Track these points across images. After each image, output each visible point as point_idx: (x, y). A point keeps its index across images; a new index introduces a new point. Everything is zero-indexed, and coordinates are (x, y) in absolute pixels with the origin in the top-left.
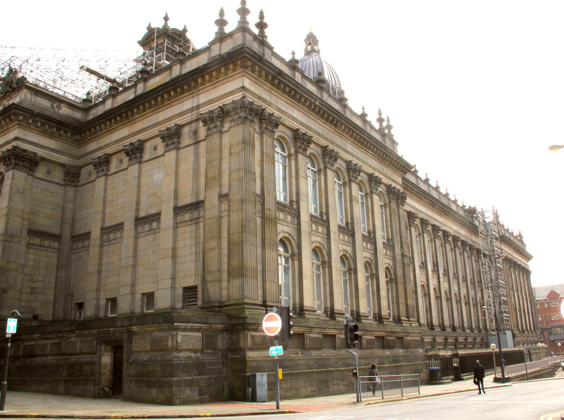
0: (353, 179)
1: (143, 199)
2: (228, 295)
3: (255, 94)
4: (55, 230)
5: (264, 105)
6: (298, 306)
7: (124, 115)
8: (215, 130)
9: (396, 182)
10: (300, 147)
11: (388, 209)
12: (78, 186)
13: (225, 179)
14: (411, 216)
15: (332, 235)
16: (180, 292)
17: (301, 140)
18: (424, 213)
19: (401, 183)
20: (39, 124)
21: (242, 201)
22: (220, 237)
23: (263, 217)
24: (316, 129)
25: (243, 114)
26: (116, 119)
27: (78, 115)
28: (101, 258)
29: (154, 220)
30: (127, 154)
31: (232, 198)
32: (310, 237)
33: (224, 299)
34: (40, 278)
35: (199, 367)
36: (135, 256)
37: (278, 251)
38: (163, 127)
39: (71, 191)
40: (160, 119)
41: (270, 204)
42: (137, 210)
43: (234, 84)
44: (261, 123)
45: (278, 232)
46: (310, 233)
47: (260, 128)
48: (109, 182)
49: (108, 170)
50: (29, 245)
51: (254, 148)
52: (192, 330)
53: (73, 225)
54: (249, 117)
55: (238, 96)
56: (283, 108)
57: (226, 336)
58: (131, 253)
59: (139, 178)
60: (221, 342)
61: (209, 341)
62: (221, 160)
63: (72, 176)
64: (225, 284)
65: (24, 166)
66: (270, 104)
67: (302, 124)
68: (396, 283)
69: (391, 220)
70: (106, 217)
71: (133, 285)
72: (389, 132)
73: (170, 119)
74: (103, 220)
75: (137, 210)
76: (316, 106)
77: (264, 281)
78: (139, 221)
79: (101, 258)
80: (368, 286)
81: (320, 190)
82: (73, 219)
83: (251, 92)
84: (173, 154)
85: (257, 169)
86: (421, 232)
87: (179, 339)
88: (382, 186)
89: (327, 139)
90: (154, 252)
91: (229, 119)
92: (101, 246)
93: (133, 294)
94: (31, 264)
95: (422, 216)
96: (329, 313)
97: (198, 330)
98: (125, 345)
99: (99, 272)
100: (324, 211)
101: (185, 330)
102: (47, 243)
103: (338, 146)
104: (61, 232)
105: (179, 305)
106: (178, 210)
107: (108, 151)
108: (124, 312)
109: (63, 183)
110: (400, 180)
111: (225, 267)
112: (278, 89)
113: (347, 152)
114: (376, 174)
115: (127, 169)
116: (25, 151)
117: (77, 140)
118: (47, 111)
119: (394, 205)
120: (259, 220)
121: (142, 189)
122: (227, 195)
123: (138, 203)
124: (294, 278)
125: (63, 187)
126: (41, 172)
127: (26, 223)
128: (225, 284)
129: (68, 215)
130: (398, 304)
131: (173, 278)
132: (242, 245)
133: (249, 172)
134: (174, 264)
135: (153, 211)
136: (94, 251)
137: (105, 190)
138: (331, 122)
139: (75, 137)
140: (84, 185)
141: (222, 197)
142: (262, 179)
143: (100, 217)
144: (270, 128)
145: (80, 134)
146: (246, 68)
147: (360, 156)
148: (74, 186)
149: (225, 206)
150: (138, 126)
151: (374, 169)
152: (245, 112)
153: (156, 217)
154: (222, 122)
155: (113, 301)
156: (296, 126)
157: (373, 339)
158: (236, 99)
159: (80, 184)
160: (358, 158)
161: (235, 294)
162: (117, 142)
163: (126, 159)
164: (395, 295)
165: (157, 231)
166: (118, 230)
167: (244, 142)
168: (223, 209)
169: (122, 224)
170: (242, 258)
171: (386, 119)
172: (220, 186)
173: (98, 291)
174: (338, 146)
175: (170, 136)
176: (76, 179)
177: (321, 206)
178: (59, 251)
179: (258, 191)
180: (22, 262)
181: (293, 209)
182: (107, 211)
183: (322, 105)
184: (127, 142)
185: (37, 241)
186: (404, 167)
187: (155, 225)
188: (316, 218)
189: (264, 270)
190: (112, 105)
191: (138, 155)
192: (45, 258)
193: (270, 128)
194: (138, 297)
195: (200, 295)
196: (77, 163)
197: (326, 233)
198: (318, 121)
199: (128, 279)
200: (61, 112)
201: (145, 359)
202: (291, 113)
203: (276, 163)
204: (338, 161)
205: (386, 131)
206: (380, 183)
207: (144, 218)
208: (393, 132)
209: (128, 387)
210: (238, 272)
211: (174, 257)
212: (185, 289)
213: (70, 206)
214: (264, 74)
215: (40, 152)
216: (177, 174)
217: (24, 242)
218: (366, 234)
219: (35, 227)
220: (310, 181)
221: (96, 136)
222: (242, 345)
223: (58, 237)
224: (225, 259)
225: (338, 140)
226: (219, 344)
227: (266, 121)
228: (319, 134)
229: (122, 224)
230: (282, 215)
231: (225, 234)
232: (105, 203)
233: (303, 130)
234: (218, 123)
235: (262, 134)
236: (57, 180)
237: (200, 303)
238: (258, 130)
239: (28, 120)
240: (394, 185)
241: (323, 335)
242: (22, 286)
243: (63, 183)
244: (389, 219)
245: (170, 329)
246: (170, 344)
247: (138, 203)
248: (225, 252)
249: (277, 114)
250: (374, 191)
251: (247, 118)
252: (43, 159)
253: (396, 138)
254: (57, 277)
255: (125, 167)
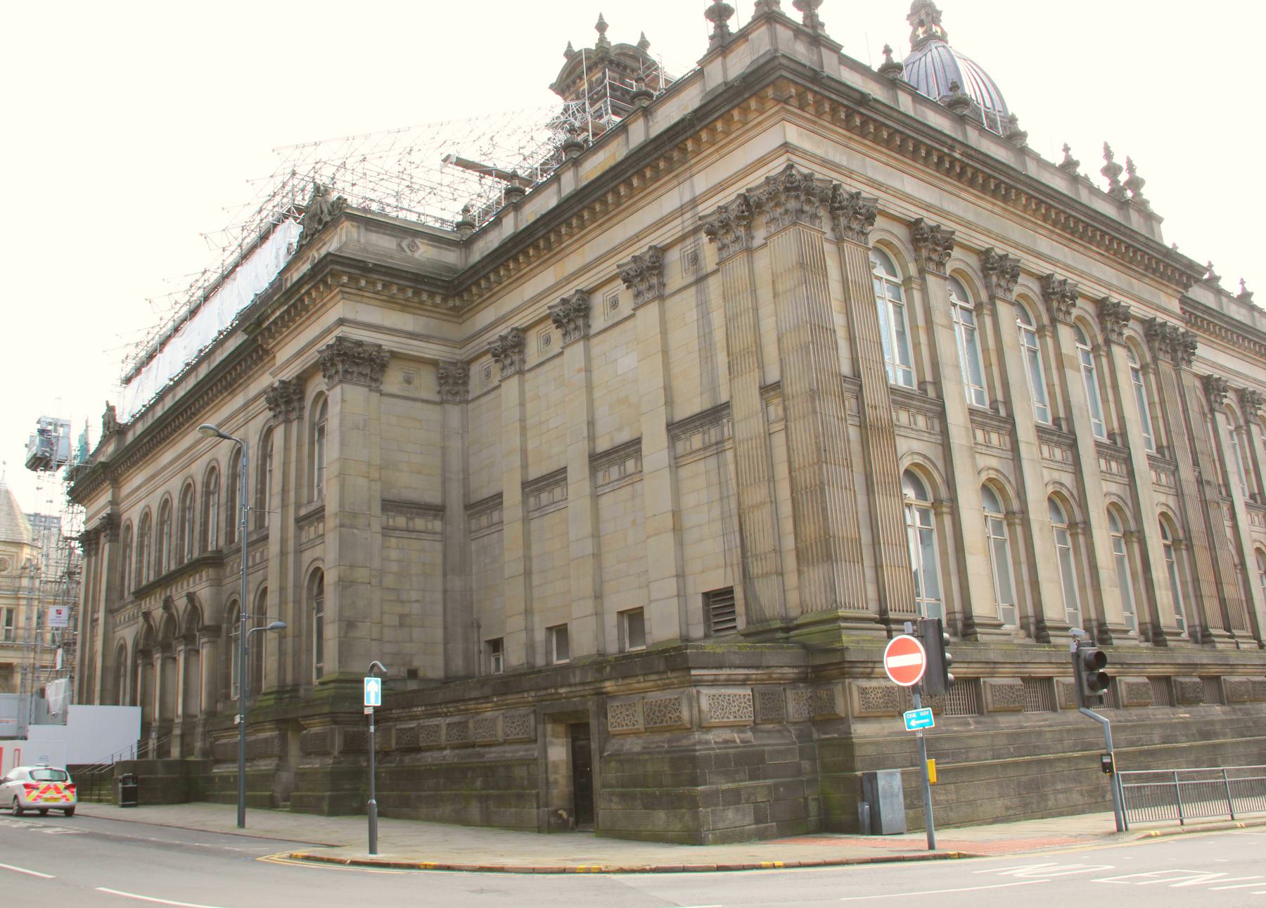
0: (1061, 316)
1: (602, 412)
2: (802, 603)
3: (814, 156)
4: (433, 497)
5: (836, 178)
6: (959, 616)
7: (542, 243)
8: (736, 247)
9: (1165, 311)
10: (930, 259)
11: (1152, 377)
12: (467, 402)
13: (771, 352)
14: (1211, 386)
15: (1023, 449)
16: (697, 603)
17: (928, 242)
18: (1246, 377)
19: (1178, 311)
20: (379, 287)
21: (813, 394)
22: (772, 479)
23: (863, 426)
24: (961, 214)
25: (792, 204)
26: (526, 254)
27: (451, 257)
28: (527, 545)
29: (628, 456)
30: (558, 323)
31: (788, 390)
32: (973, 458)
33: (794, 612)
34: (414, 595)
35: (749, 762)
36: (596, 535)
37: (902, 496)
38: (625, 257)
39: (454, 412)
40: (617, 241)
41: (875, 394)
42: (592, 438)
43: (766, 142)
44: (834, 218)
45: (899, 455)
46: (973, 450)
47: (833, 230)
48: (528, 386)
49: (523, 361)
50: (387, 531)
51: (826, 275)
52: (729, 682)
53: (465, 482)
54: (806, 208)
55: (776, 167)
56: (880, 178)
57: (804, 691)
58: (587, 529)
59: (588, 370)
60: (795, 705)
61: (768, 707)
62: (756, 310)
63: (453, 381)
64: (792, 580)
65: (360, 374)
66: (850, 173)
67: (928, 207)
68: (1190, 548)
69: (1162, 402)
70: (530, 459)
71: (598, 596)
72: (1137, 194)
73: (638, 237)
74: (525, 467)
75: (592, 438)
76: (953, 161)
77: (878, 567)
78: (597, 460)
79: (527, 545)
80: (1120, 561)
81: (985, 350)
82: (465, 470)
83: (805, 154)
84: (652, 310)
85: (839, 320)
86: (1242, 422)
87: (704, 704)
88: (1131, 323)
89: (987, 233)
90: (634, 523)
91: (764, 219)
92: (526, 520)
93: (599, 614)
94: (394, 567)
95: (1239, 383)
96: (1032, 628)
97: (743, 683)
98: (593, 722)
99: (528, 573)
100: (1000, 397)
101: (714, 683)
102: (419, 523)
103: (1017, 246)
104: (444, 500)
105: (698, 631)
106: (676, 429)
107: (519, 321)
108: (585, 653)
109: (437, 398)
110: (1175, 306)
111: (789, 542)
112: (864, 137)
113: (1039, 255)
114: (1115, 298)
115: (561, 353)
116: (359, 344)
117: (454, 308)
118: (391, 257)
119: (1165, 366)
120: (853, 433)
121: (597, 394)
122: (777, 386)
123: (591, 424)
124: (944, 553)
125: (438, 408)
126: (393, 380)
127: (377, 487)
128: (792, 580)
129: (455, 463)
130: (1199, 597)
131: (681, 575)
132: (822, 490)
133: (821, 329)
134: (680, 544)
135: (625, 436)
136: (512, 531)
137: (522, 404)
138: (994, 194)
139: (451, 303)
140: (479, 397)
141: (769, 390)
142: (852, 340)
143: (516, 461)
144: (855, 225)
145: (460, 295)
146: (786, 102)
147: (1070, 262)
148: (460, 402)
149: (775, 410)
150: (573, 262)
151: (1109, 286)
152: (797, 197)
153: (633, 447)
154: (749, 228)
155: (561, 632)
156: (914, 213)
157: (1145, 684)
158: (773, 173)
159: (470, 397)
160: (1067, 267)
161: (817, 602)
162: (535, 300)
163: (556, 334)
164: (1189, 578)
165: (637, 478)
166: (557, 483)
167: (801, 265)
168: (772, 417)
169: (564, 470)
170: (825, 519)
171: (1125, 167)
172: (762, 367)
173: (528, 612)
174: (1017, 246)
175: (641, 273)
176: (461, 388)
177: (991, 388)
178: (444, 537)
179: (846, 369)
180: (376, 564)
181: (928, 399)
182: (531, 446)
183: (969, 157)
184: (555, 299)
185: (401, 521)
186: (1182, 274)
187: (630, 465)
188: (983, 414)
189: (875, 543)
190: (516, 225)
191: (580, 322)
192: (419, 553)
193: (855, 225)
194: (611, 620)
195: (740, 607)
196: (461, 354)
197: (1009, 446)
198: (963, 195)
199: (585, 585)
200: (417, 255)
201: (637, 749)
202: (898, 185)
203: (879, 303)
204: (1020, 280)
205: (1129, 194)
206: (1127, 317)
207: (607, 453)
208: (1146, 192)
209: (606, 807)
210: (820, 550)
211: (678, 529)
212: (707, 596)
213: (455, 444)
214: (827, 108)
215: (388, 342)
216: (665, 352)
217: (376, 526)
218: (1105, 440)
219: (393, 494)
220: (960, 333)
221: (491, 296)
222: (840, 709)
223: (438, 511)
224: (788, 526)
225: (1016, 231)
226: (790, 709)
227: (848, 212)
228: (968, 224)
229: (564, 470)
230: (903, 417)
231: (782, 471)
232: (523, 430)
233: (931, 220)
234: (741, 232)
235: (839, 241)
236: (424, 395)
237: (741, 623)
238: (829, 235)
239: (358, 281)
240: (1161, 317)
241: (1023, 679)
242: (382, 613)
243: (437, 398)
244: (1156, 399)
245: (682, 684)
246: (685, 714)
247: (591, 424)
248: (786, 509)
249: (867, 192)
250: (1114, 337)
251: (802, 211)
252: (394, 355)
253: (1154, 207)
254: (445, 591)
255: (557, 350)
